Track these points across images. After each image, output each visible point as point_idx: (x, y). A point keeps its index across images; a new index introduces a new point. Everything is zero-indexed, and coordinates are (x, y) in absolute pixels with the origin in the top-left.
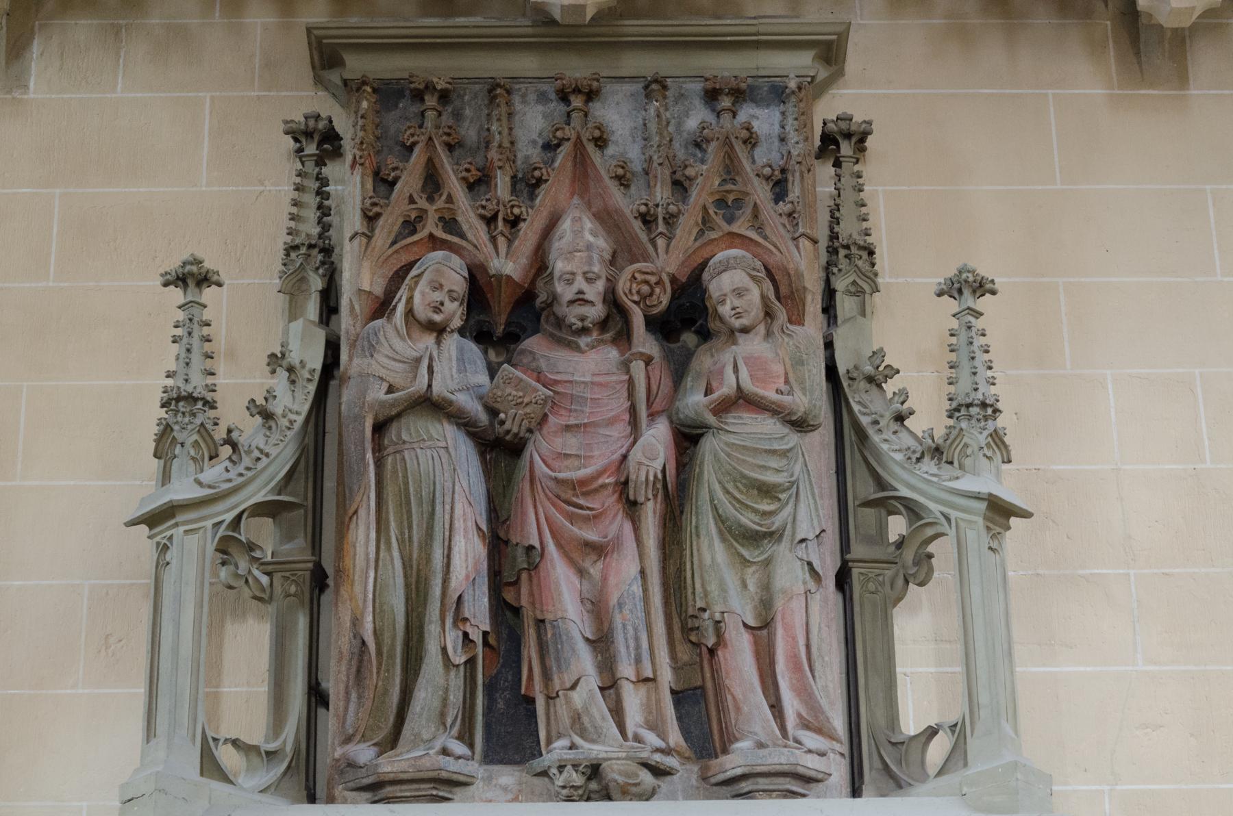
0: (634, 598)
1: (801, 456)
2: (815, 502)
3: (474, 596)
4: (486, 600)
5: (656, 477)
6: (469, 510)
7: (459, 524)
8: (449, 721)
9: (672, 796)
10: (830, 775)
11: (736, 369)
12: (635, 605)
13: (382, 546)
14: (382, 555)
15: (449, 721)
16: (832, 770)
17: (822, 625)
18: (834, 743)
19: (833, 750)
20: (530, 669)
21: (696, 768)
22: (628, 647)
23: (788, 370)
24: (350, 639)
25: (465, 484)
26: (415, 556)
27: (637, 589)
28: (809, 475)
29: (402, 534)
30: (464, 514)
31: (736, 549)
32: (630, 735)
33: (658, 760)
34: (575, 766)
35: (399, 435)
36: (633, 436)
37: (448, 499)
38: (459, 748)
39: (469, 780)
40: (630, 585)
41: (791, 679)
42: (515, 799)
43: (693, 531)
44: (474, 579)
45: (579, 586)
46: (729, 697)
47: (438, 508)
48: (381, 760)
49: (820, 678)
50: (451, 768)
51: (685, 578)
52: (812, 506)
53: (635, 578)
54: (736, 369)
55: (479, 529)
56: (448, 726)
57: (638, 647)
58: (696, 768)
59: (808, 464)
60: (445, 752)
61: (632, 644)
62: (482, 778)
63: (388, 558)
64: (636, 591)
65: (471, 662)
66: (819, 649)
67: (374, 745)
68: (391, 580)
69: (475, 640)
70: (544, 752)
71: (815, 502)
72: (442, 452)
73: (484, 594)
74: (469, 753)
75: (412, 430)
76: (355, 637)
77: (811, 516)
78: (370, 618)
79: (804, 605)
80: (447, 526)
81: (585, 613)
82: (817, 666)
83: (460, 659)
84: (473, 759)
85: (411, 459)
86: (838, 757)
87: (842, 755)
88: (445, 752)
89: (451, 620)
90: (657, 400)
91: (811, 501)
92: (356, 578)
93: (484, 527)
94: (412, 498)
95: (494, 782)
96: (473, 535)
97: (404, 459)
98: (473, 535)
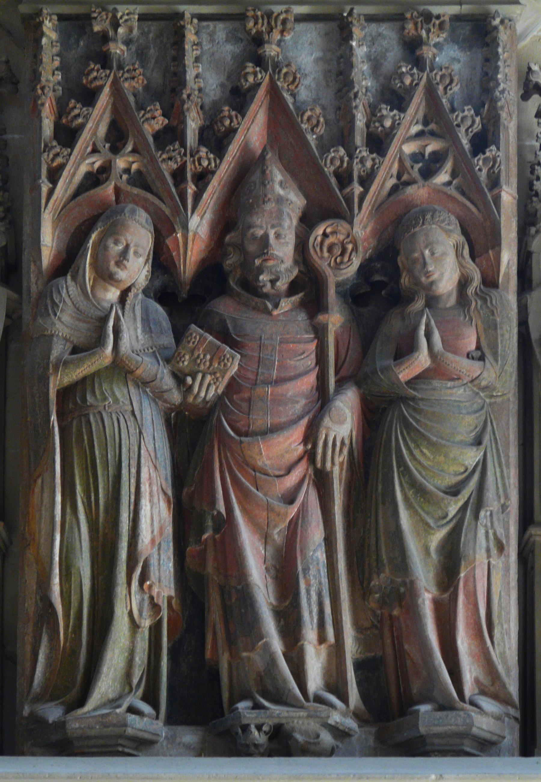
0: (318, 564)
1: (489, 424)
2: (502, 472)
3: (159, 560)
4: (171, 565)
5: (343, 443)
6: (153, 474)
7: (145, 488)
8: (135, 681)
9: (350, 753)
10: (504, 738)
11: (428, 335)
12: (319, 571)
13: (68, 510)
14: (68, 518)
15: (135, 681)
16: (506, 733)
17: (502, 594)
18: (509, 707)
19: (508, 715)
20: (215, 634)
21: (373, 730)
22: (311, 612)
23: (480, 334)
24: (36, 602)
25: (151, 448)
26: (101, 519)
27: (321, 556)
28: (496, 443)
29: (88, 497)
30: (150, 478)
31: (420, 516)
32: (311, 697)
33: (338, 720)
34: (259, 728)
35: (84, 400)
36: (320, 402)
37: (134, 463)
38: (146, 708)
39: (154, 738)
40: (314, 551)
41: (469, 644)
42: (200, 755)
43: (380, 497)
44: (160, 544)
45: (263, 552)
46: (408, 662)
47: (125, 471)
48: (70, 717)
49: (499, 644)
50: (138, 726)
51: (369, 546)
52: (498, 475)
53: (320, 545)
54: (428, 335)
55: (165, 493)
56: (134, 687)
57: (321, 612)
58: (373, 730)
59: (496, 432)
60: (132, 710)
61: (315, 609)
62: (166, 737)
63: (74, 520)
64: (320, 557)
65: (156, 629)
66: (499, 617)
67: (61, 703)
68: (78, 543)
69: (160, 603)
70: (226, 712)
71: (502, 472)
72: (128, 416)
73: (169, 558)
74: (153, 712)
75: (97, 392)
76: (41, 600)
77: (497, 484)
78: (56, 580)
79: (486, 573)
80: (133, 490)
81: (269, 579)
82: (497, 632)
83: (146, 623)
84: (157, 718)
85: (96, 422)
86: (512, 721)
87: (516, 719)
88: (132, 710)
89: (137, 584)
90: (345, 365)
91: (498, 470)
92: (42, 541)
93: (170, 492)
94: (98, 461)
95: (178, 740)
96: (159, 499)
97: (89, 423)
98: (159, 499)
